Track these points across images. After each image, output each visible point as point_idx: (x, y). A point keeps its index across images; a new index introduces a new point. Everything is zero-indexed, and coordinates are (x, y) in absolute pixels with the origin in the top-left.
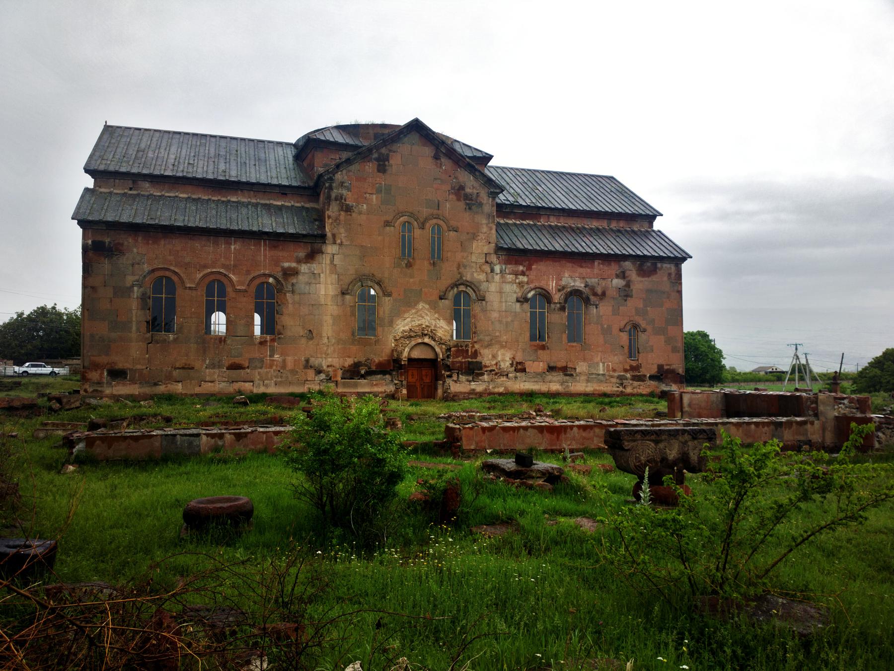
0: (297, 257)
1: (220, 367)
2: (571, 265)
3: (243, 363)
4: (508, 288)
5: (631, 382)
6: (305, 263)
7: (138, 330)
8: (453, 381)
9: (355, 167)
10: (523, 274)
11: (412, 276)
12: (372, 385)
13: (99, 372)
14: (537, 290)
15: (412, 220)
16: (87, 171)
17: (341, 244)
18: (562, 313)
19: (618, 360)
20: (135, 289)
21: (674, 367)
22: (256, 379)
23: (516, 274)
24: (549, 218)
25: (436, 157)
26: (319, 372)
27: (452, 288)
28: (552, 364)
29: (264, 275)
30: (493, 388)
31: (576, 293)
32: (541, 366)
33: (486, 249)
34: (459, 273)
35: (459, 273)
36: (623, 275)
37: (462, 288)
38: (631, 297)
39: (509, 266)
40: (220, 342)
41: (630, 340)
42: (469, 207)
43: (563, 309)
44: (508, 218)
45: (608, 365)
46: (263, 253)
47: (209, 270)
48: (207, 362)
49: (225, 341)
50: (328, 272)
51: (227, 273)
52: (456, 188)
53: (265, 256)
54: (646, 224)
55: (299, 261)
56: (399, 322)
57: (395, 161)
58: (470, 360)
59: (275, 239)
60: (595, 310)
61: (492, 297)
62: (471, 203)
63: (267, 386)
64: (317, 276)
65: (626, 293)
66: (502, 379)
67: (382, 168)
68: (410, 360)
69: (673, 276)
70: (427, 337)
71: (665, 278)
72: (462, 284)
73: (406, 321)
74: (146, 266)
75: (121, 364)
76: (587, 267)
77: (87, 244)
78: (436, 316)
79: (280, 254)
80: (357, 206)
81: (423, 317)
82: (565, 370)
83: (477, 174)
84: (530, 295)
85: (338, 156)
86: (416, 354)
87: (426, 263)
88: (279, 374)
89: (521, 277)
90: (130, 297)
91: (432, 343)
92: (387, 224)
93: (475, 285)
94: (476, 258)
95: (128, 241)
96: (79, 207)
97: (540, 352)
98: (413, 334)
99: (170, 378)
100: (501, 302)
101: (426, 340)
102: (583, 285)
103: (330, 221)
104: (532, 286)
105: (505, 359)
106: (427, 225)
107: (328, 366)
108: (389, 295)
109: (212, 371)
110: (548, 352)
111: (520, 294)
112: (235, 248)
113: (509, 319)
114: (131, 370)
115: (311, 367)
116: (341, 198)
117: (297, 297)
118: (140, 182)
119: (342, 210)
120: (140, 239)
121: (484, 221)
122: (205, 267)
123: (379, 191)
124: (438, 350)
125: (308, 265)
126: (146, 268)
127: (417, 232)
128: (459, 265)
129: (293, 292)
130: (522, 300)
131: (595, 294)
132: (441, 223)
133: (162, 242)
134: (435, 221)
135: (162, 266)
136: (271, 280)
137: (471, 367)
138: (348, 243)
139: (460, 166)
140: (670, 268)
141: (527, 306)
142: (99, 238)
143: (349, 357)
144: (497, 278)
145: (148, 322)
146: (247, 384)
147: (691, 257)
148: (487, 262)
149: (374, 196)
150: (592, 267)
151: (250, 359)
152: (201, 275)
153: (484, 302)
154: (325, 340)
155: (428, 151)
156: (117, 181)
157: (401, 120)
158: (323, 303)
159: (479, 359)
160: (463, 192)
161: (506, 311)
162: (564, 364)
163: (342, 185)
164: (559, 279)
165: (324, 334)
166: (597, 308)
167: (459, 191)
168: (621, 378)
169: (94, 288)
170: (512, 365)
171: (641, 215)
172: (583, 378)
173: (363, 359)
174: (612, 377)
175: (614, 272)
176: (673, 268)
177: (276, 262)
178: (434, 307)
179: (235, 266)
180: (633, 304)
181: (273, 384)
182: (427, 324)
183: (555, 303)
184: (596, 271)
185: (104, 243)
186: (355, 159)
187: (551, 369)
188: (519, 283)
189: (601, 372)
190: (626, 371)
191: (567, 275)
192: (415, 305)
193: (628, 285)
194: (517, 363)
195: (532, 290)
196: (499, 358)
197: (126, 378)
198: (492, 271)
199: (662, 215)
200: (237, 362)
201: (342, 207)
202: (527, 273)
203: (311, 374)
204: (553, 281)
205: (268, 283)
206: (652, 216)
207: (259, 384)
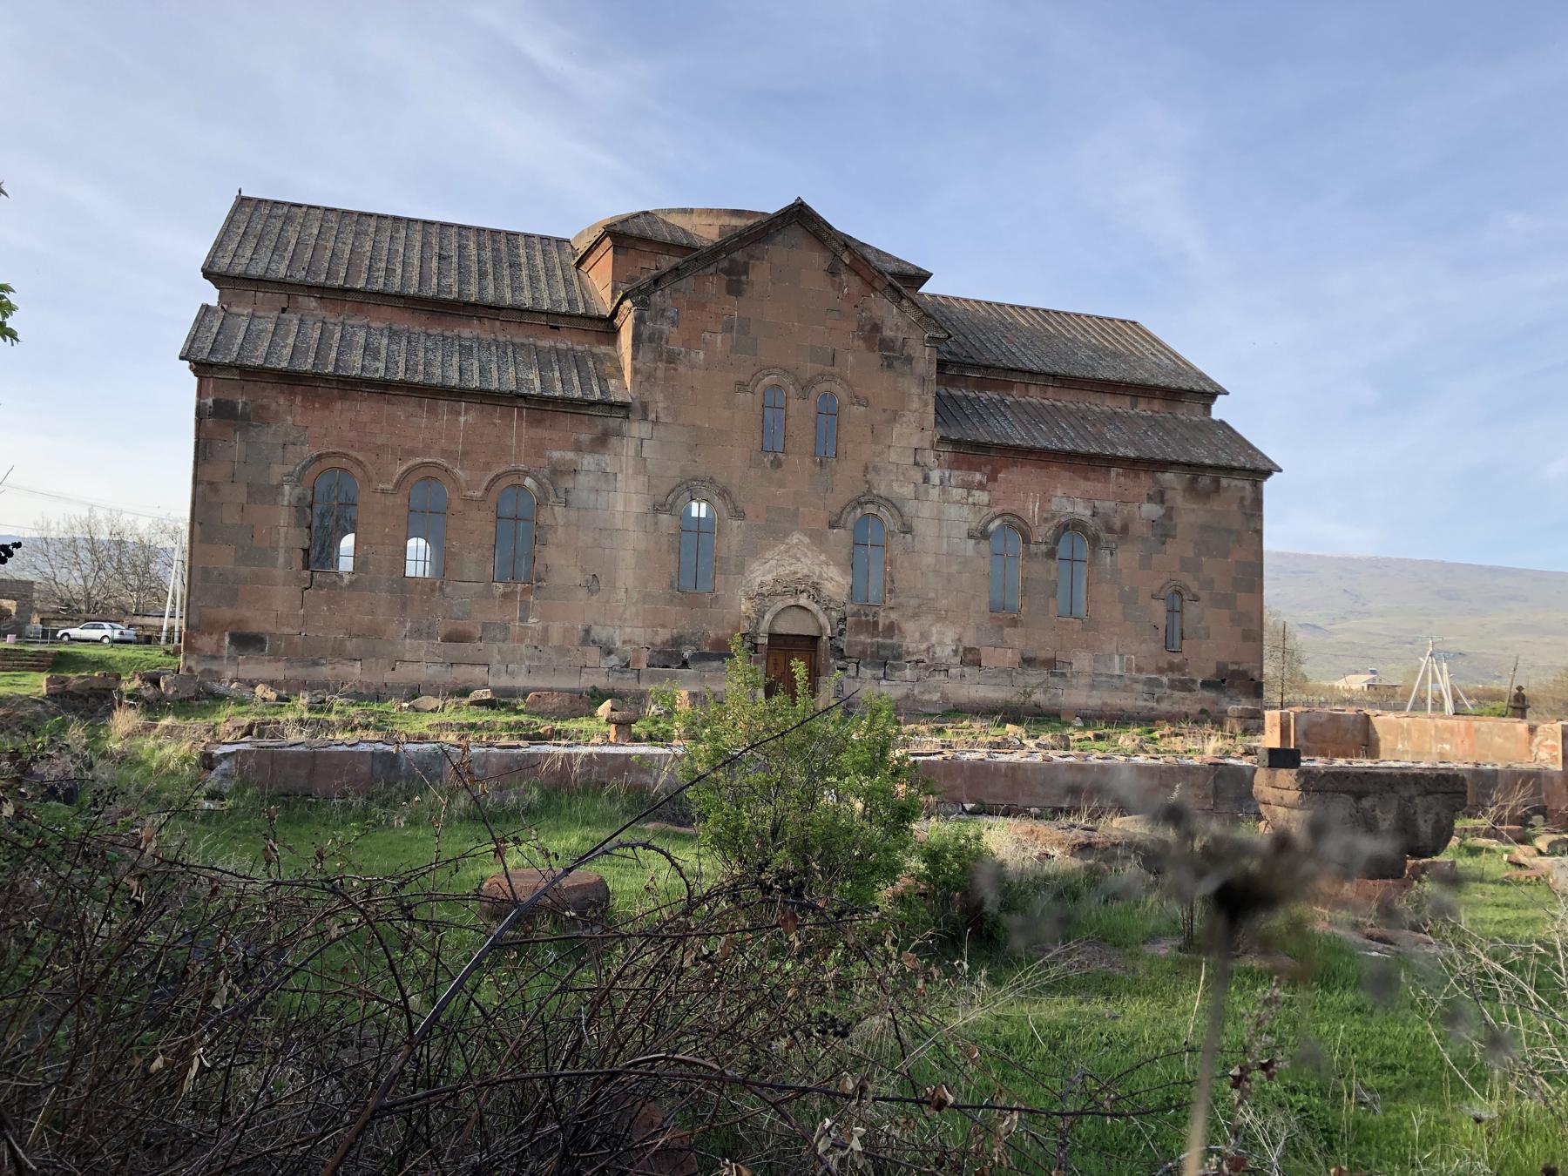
0: (577, 441)
1: (429, 636)
2: (1067, 474)
3: (472, 629)
4: (952, 511)
5: (1168, 691)
6: (593, 451)
7: (288, 563)
8: (849, 677)
9: (687, 283)
10: (981, 487)
11: (781, 485)
12: (703, 680)
13: (215, 637)
14: (1006, 517)
15: (787, 380)
16: (207, 274)
17: (656, 422)
18: (1050, 562)
19: (1147, 649)
20: (287, 488)
21: (1244, 667)
22: (495, 662)
23: (968, 487)
24: (1027, 389)
25: (833, 272)
26: (610, 652)
27: (854, 508)
28: (1029, 654)
29: (516, 472)
30: (922, 693)
31: (1073, 526)
32: (1009, 657)
33: (915, 442)
34: (867, 482)
35: (867, 482)
36: (1159, 497)
37: (871, 509)
38: (1174, 538)
39: (956, 473)
40: (433, 590)
42: (889, 364)
43: (1051, 554)
44: (953, 386)
45: (1128, 659)
46: (516, 431)
47: (418, 460)
48: (408, 625)
49: (441, 589)
50: (630, 471)
51: (450, 467)
52: (867, 328)
53: (519, 436)
54: (1199, 408)
55: (578, 448)
56: (755, 566)
57: (760, 274)
58: (880, 640)
59: (542, 406)
60: (1109, 558)
61: (925, 529)
62: (891, 355)
63: (512, 674)
64: (611, 477)
65: (1164, 530)
66: (937, 678)
67: (735, 289)
68: (772, 636)
69: (1247, 503)
70: (805, 595)
71: (1235, 507)
72: (872, 502)
73: (767, 566)
74: (306, 448)
75: (258, 623)
76: (1099, 481)
77: (205, 404)
78: (823, 557)
79: (546, 434)
80: (687, 353)
81: (798, 559)
82: (1050, 664)
83: (905, 303)
84: (992, 527)
85: (653, 264)
86: (783, 627)
87: (808, 460)
88: (537, 653)
89: (977, 493)
90: (276, 503)
91: (814, 607)
92: (741, 386)
93: (894, 505)
94: (898, 456)
95: (276, 399)
96: (192, 339)
97: (1007, 631)
98: (779, 589)
99: (339, 653)
100: (940, 537)
102: (1089, 513)
103: (639, 378)
104: (997, 510)
105: (944, 640)
106: (813, 392)
107: (624, 642)
108: (739, 514)
109: (415, 643)
110: (1020, 630)
111: (974, 525)
112: (465, 422)
113: (954, 568)
114: (272, 635)
115: (594, 642)
116: (661, 338)
117: (573, 515)
118: (300, 299)
119: (661, 360)
120: (298, 399)
121: (915, 390)
122: (412, 453)
123: (728, 328)
124: (823, 619)
125: (596, 456)
126: (309, 451)
127: (795, 405)
128: (866, 468)
129: (567, 504)
130: (984, 535)
131: (1110, 530)
132: (837, 389)
133: (338, 405)
134: (825, 386)
135: (337, 450)
136: (528, 482)
137: (882, 652)
138: (669, 420)
139: (874, 289)
140: (1244, 488)
141: (984, 545)
142: (224, 396)
143: (663, 626)
144: (934, 493)
145: (306, 551)
146: (478, 670)
147: (1280, 471)
148: (916, 464)
149: (719, 337)
150: (1107, 481)
151: (484, 624)
152: (405, 467)
153: (908, 536)
154: (621, 594)
155: (818, 259)
156: (260, 295)
157: (772, 203)
158: (619, 523)
159: (895, 640)
160: (879, 335)
161: (948, 554)
162: (1050, 655)
163: (662, 316)
164: (1046, 499)
165: (620, 584)
166: (1112, 554)
167: (872, 333)
168: (1151, 683)
169: (213, 485)
170: (956, 652)
171: (1191, 391)
172: (1083, 681)
173: (688, 630)
174: (1135, 681)
175: (1145, 491)
176: (1247, 485)
177: (539, 450)
178: (817, 538)
179: (465, 454)
181: (524, 670)
182: (805, 571)
183: (1037, 543)
184: (1112, 487)
185: (235, 406)
186: (686, 269)
187: (1028, 661)
188: (974, 504)
189: (1117, 672)
190: (1161, 671)
191: (1059, 493)
192: (786, 535)
193: (1169, 514)
194: (966, 649)
195: (996, 517)
196: (934, 640)
197: (263, 650)
198: (926, 480)
199: (1227, 393)
200: (460, 628)
201: (661, 355)
202: (990, 486)
203: (593, 654)
204: (1034, 503)
205: (522, 486)
206: (1209, 395)
207: (499, 672)
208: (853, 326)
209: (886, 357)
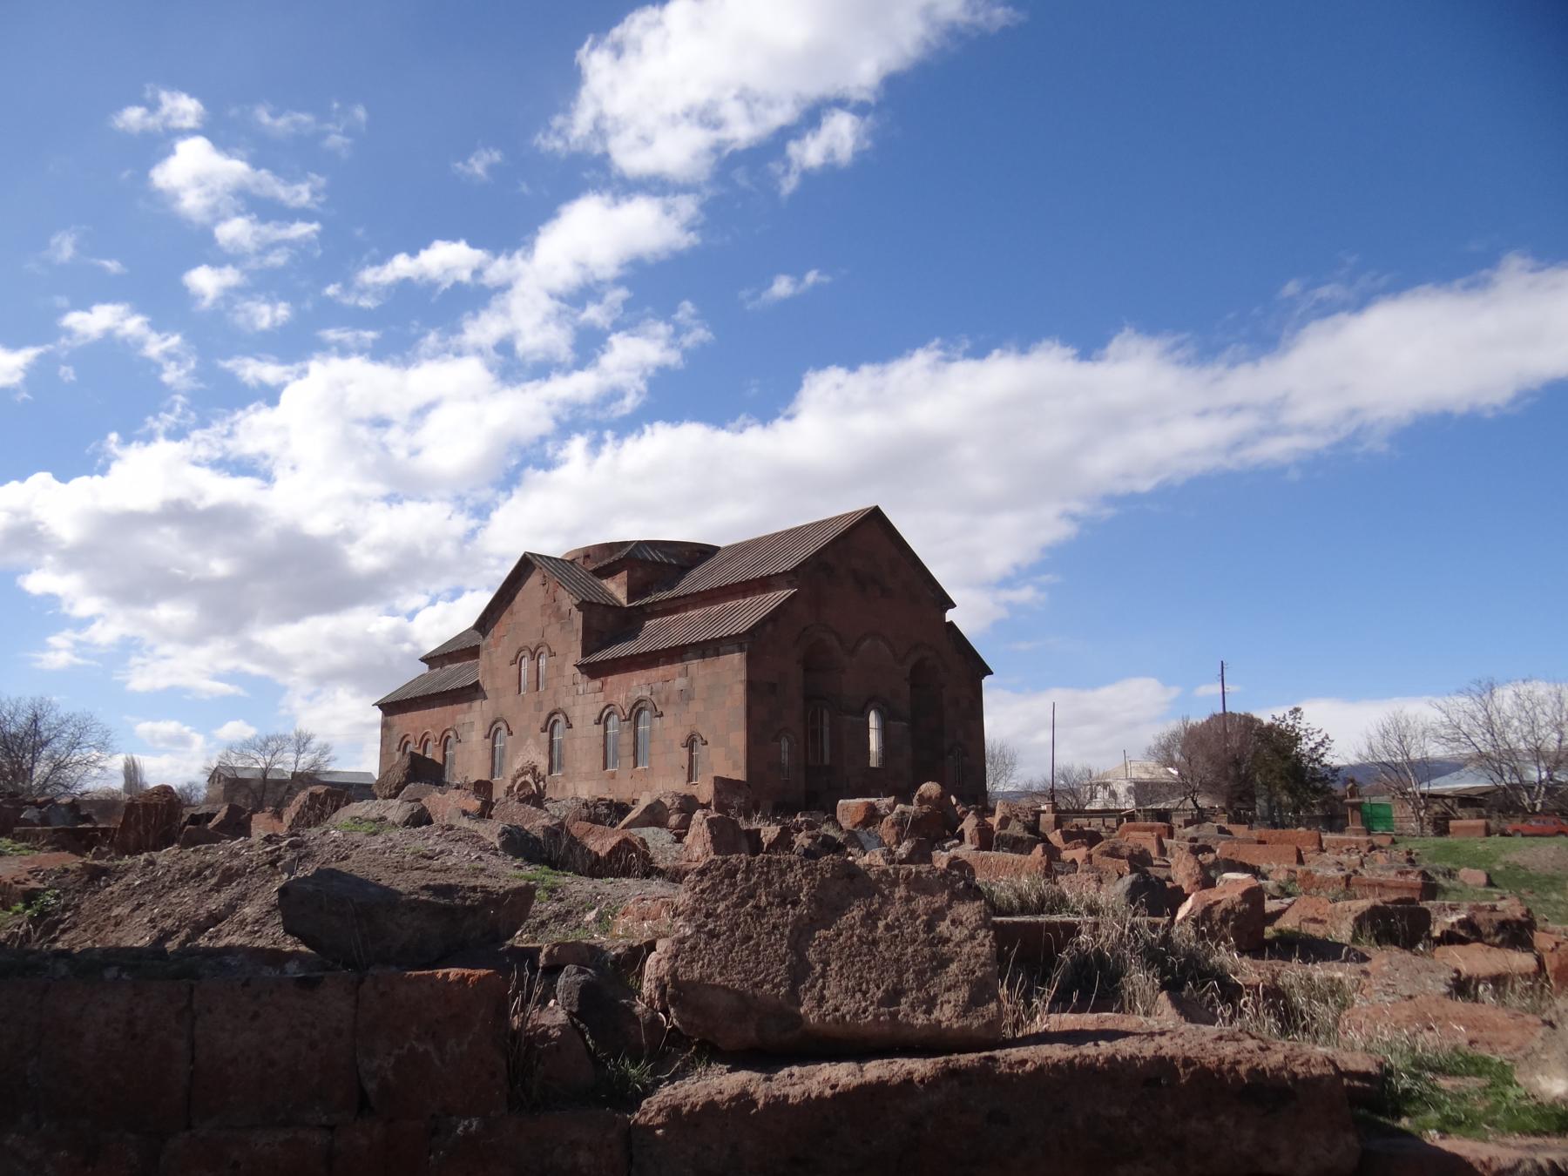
14: (612, 707)
35: (555, 702)
37: (556, 717)
38: (693, 699)
41: (691, 757)
72: (555, 713)
101: (529, 778)
102: (649, 693)
104: (606, 704)
122: (424, 729)
126: (402, 736)
131: (659, 701)
136: (451, 733)
144: (580, 699)
180: (696, 706)
182: (532, 760)
191: (635, 684)
208: (549, 611)
209: (562, 623)
